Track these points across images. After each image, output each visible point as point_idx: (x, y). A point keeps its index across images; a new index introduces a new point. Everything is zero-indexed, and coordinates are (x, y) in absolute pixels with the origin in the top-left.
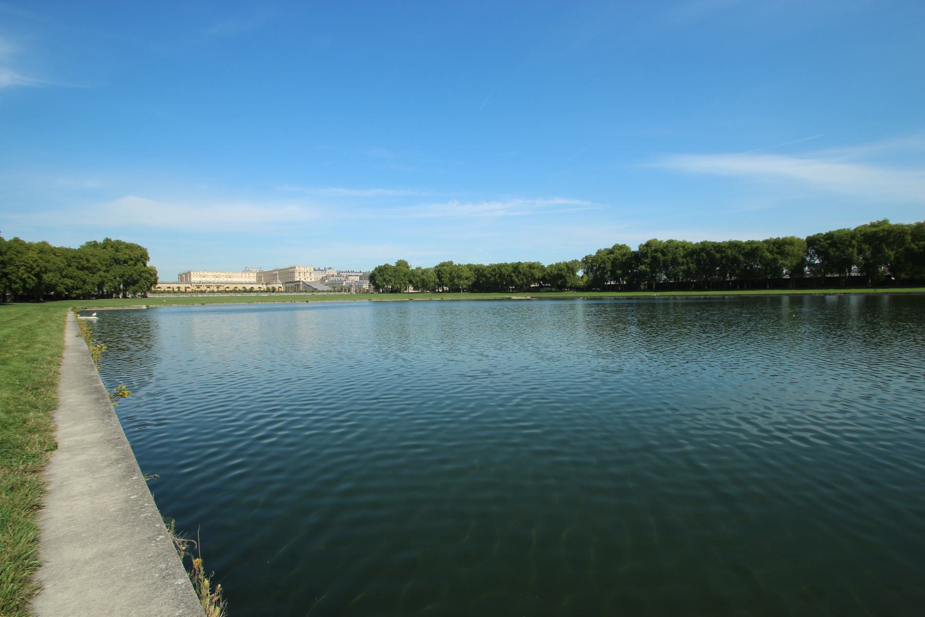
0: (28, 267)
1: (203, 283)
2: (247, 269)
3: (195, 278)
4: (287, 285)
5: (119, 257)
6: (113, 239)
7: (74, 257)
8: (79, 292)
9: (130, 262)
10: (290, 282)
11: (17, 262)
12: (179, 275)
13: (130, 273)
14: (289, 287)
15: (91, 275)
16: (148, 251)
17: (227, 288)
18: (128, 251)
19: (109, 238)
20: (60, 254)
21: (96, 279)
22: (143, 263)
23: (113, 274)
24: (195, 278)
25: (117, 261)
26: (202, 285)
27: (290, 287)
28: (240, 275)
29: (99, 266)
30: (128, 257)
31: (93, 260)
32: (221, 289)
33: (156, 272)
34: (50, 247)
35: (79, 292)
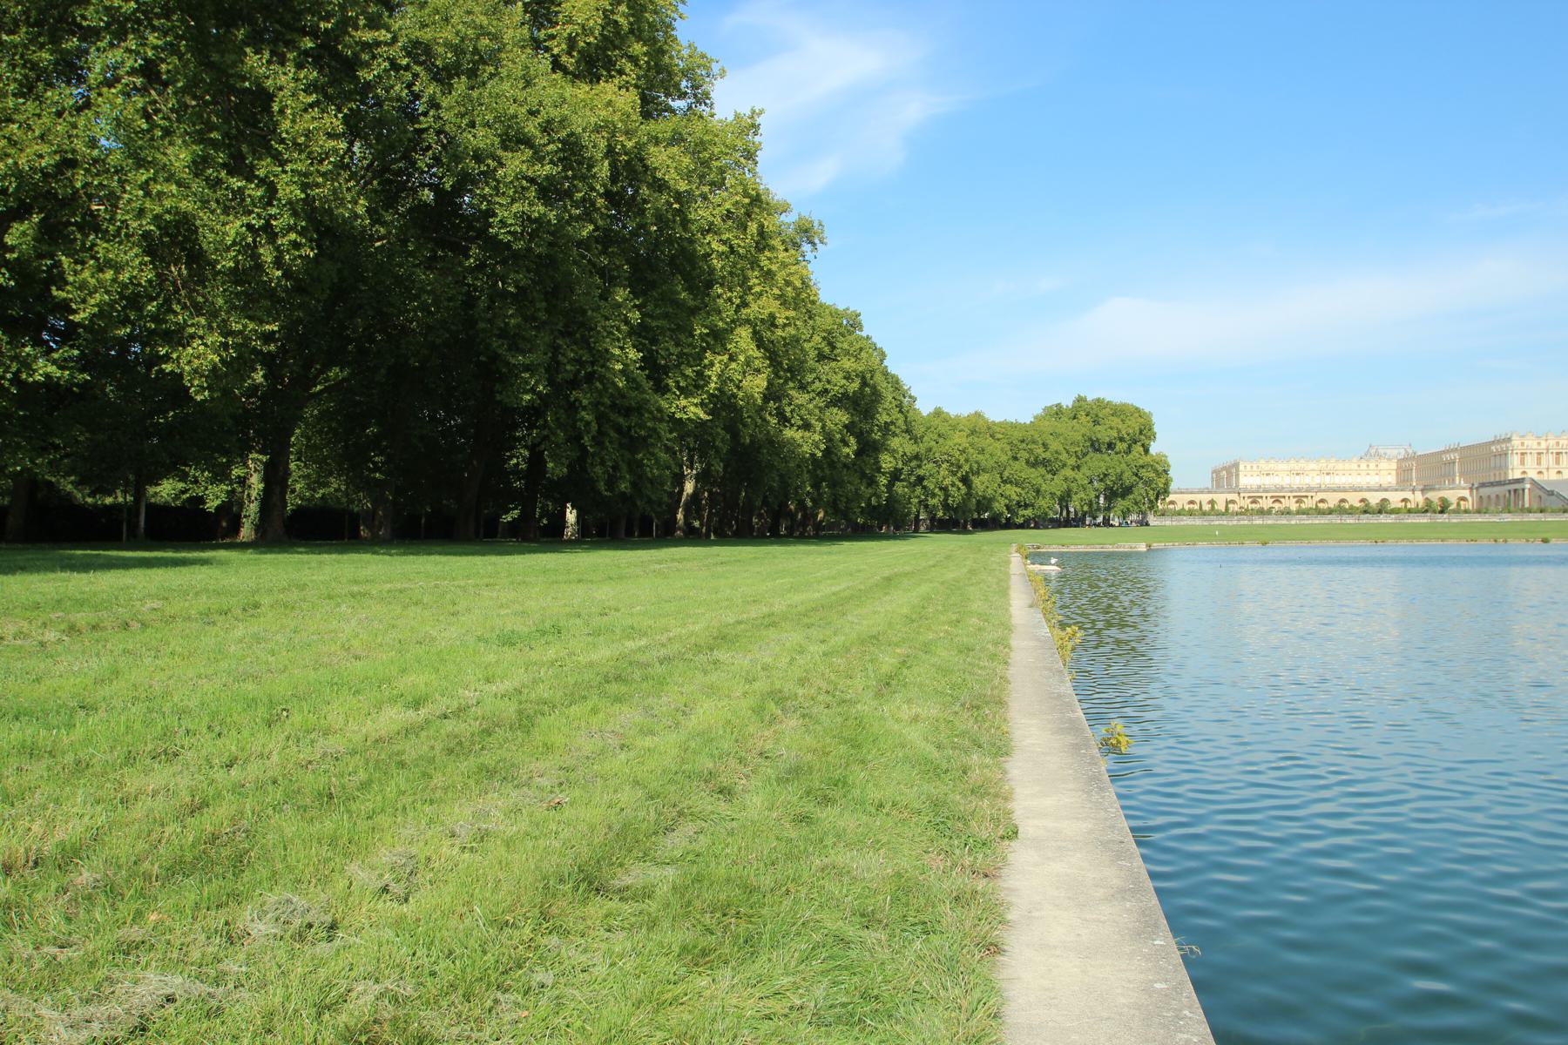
0: (952, 464)
1: (1267, 492)
2: (1373, 451)
3: (1247, 480)
4: (1485, 491)
5: (1099, 437)
6: (1091, 397)
7: (1023, 441)
8: (1029, 512)
9: (1120, 446)
10: (1492, 484)
11: (937, 455)
12: (1213, 472)
13: (1119, 471)
14: (1489, 497)
15: (1050, 476)
16: (1154, 419)
17: (1322, 501)
18: (1116, 421)
19: (1082, 395)
20: (1000, 436)
21: (1057, 485)
22: (1143, 445)
23: (1088, 473)
24: (1247, 480)
25: (1095, 446)
26: (1264, 495)
27: (1493, 497)
28: (1355, 466)
29: (1064, 456)
30: (1116, 435)
31: (1055, 445)
32: (1308, 504)
33: (1169, 466)
34: (986, 421)
35: (1029, 512)
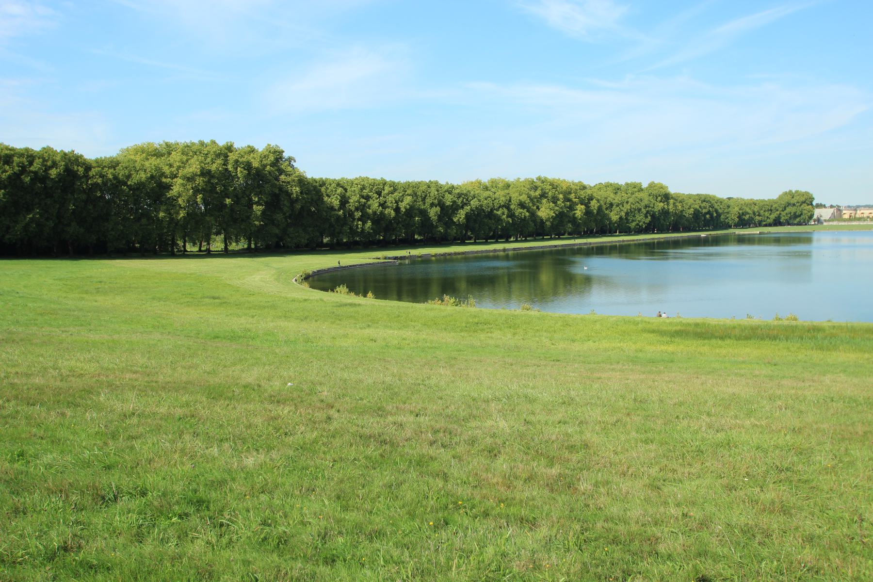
8: (764, 223)
9: (797, 204)
21: (773, 216)
25: (789, 204)
